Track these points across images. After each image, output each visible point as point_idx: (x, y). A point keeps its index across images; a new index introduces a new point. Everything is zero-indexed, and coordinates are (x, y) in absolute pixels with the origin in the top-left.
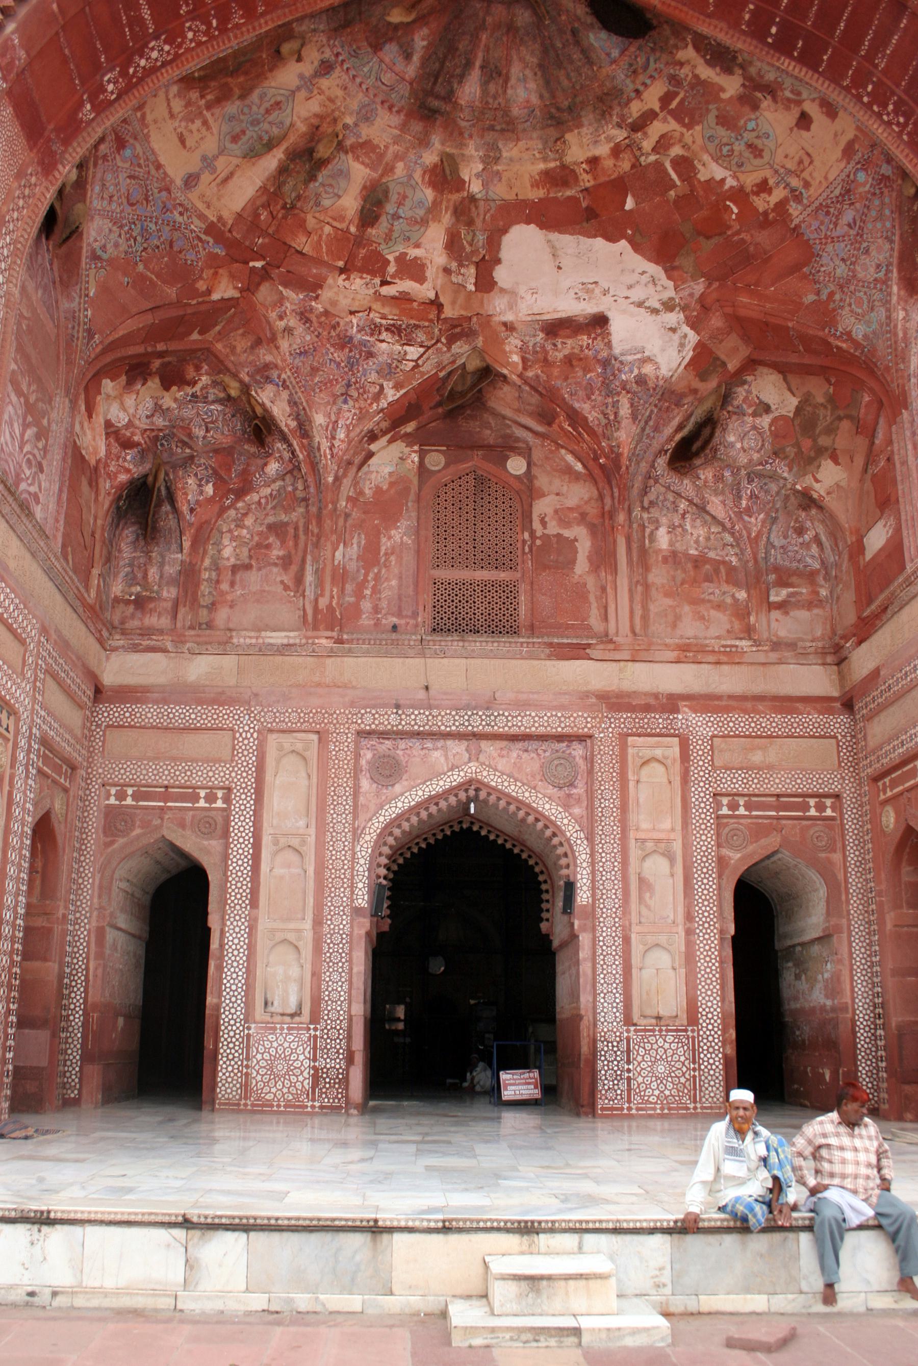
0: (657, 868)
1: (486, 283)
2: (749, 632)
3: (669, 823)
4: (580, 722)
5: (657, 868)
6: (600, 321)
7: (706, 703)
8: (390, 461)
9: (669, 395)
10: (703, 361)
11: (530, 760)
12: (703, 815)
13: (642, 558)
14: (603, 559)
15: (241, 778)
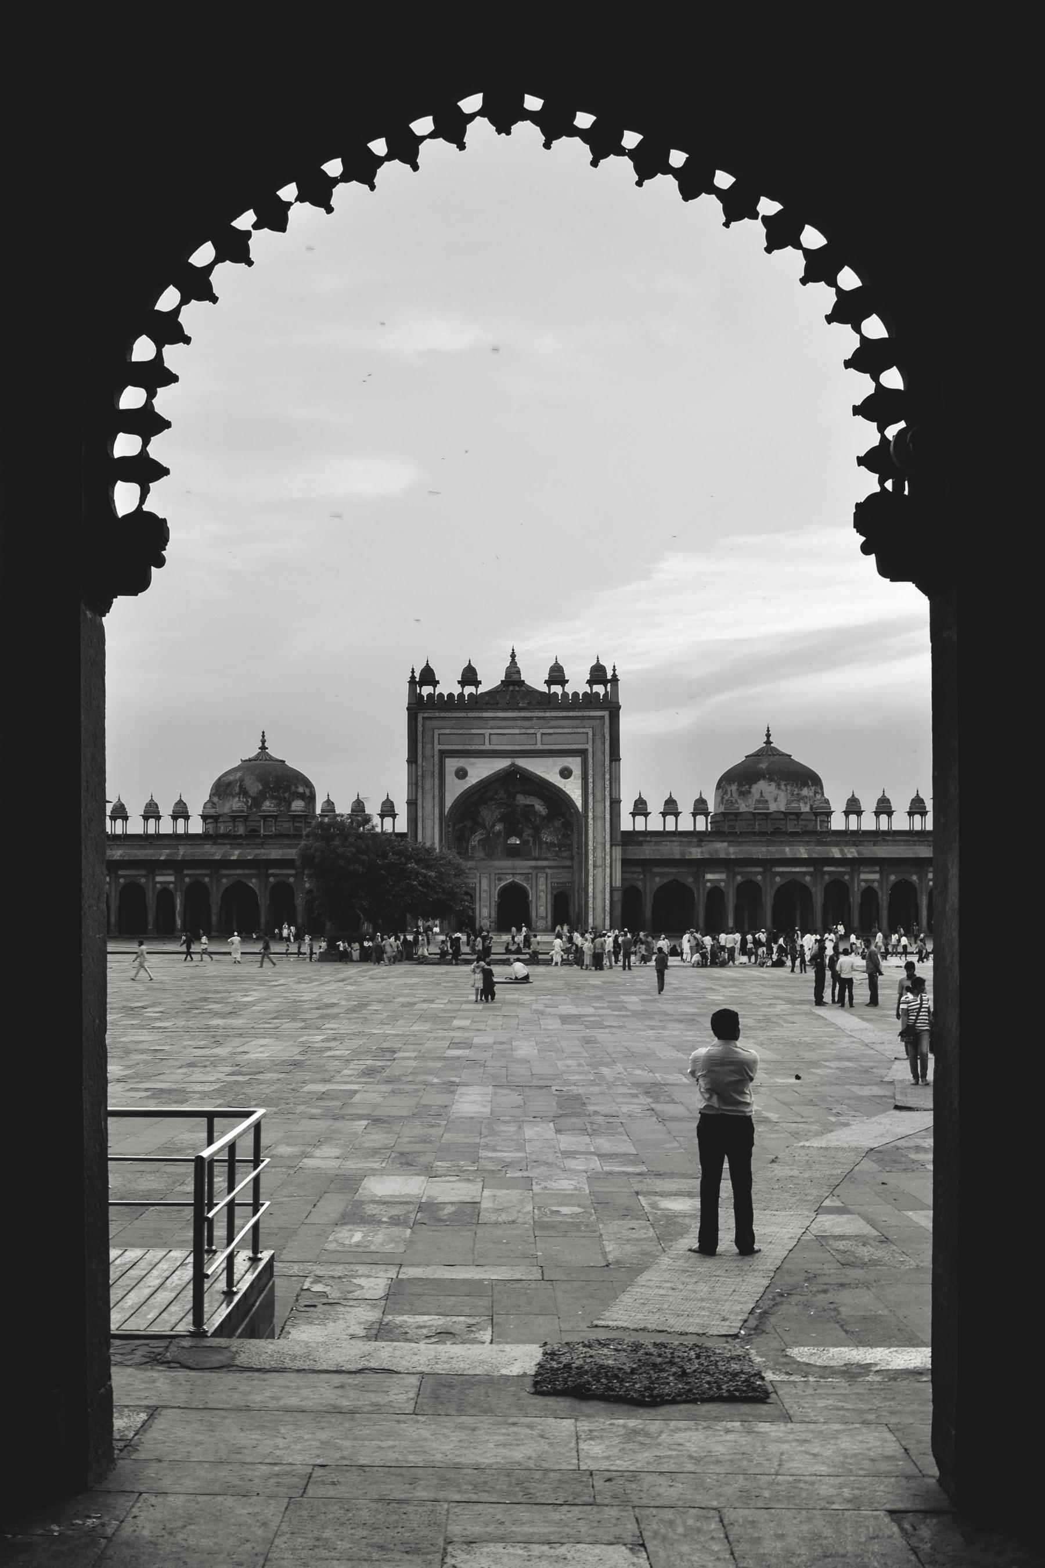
0: (542, 894)
1: (514, 799)
2: (557, 856)
3: (544, 887)
4: (530, 871)
5: (542, 894)
6: (533, 806)
7: (550, 867)
8: (498, 827)
9: (544, 818)
10: (549, 814)
11: (523, 877)
12: (549, 885)
13: (541, 843)
14: (534, 843)
15: (477, 881)
